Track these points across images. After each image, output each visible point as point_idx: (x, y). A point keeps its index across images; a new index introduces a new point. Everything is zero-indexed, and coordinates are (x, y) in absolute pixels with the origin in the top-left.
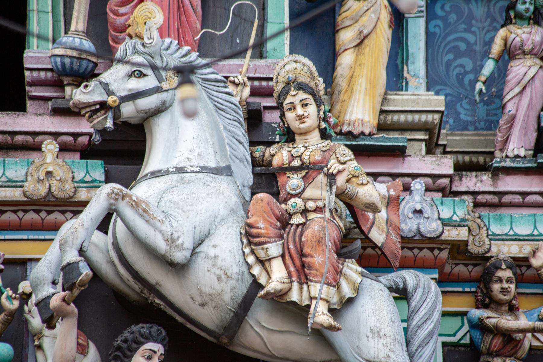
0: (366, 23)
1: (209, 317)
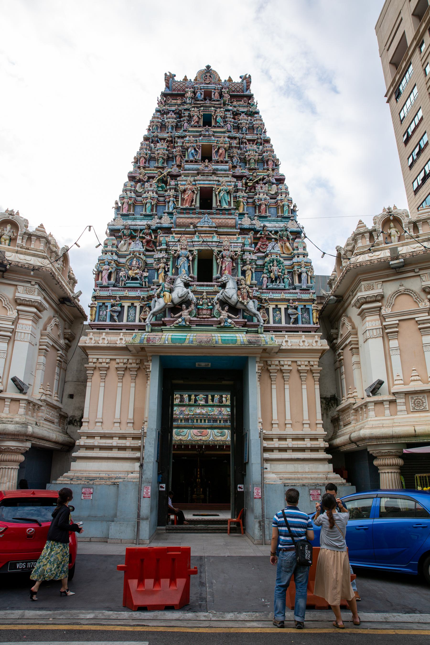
0: (249, 273)
1: (233, 304)
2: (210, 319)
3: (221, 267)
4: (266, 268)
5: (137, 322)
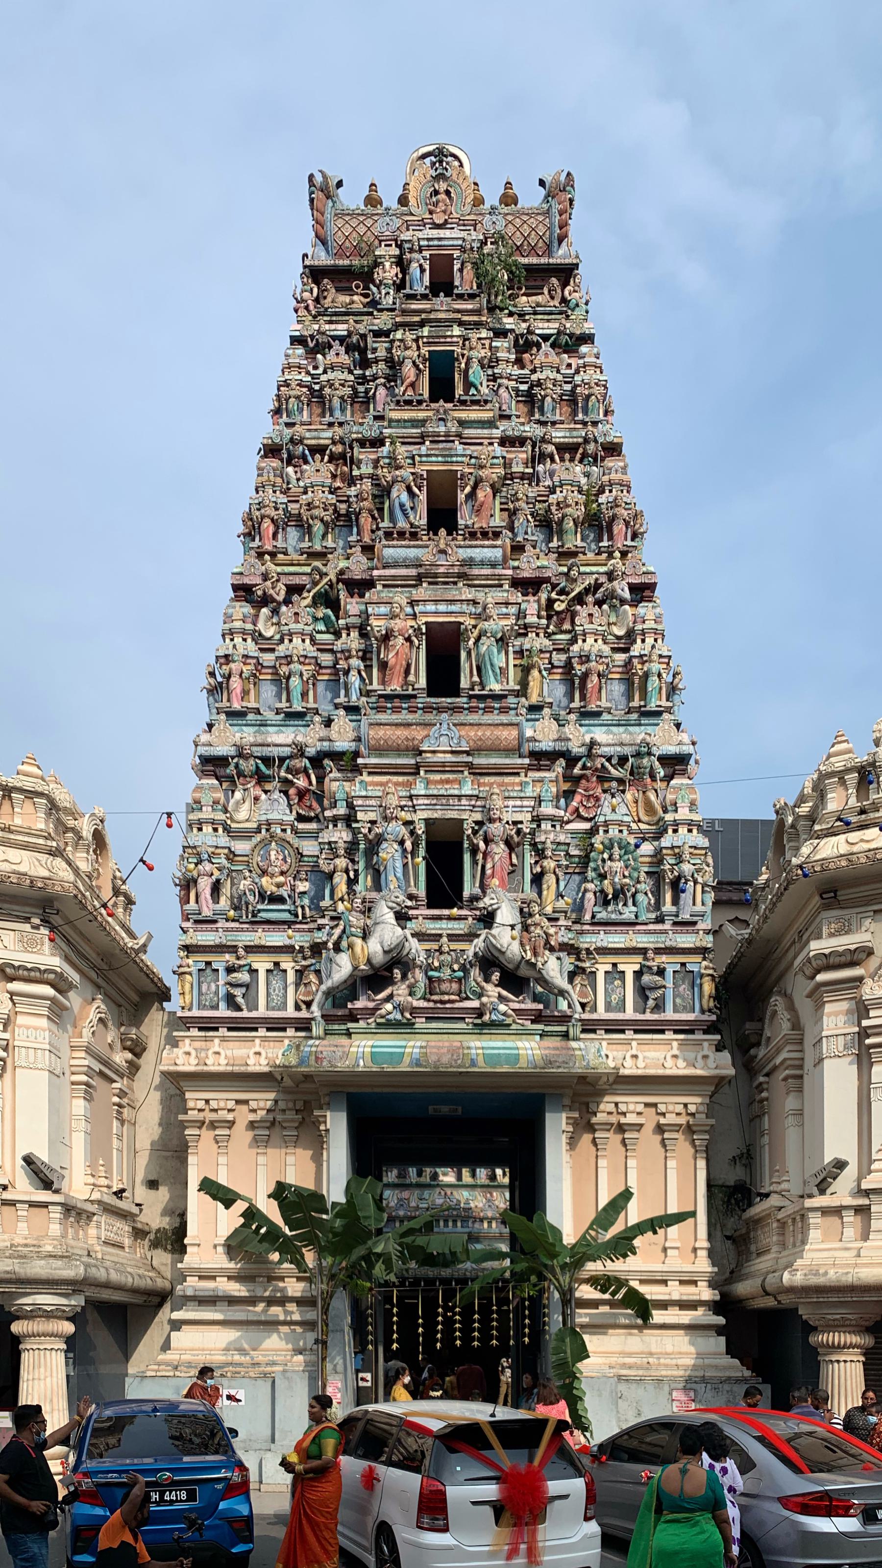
2: (457, 1005)
3: (483, 867)
4: (592, 865)
5: (290, 1012)
